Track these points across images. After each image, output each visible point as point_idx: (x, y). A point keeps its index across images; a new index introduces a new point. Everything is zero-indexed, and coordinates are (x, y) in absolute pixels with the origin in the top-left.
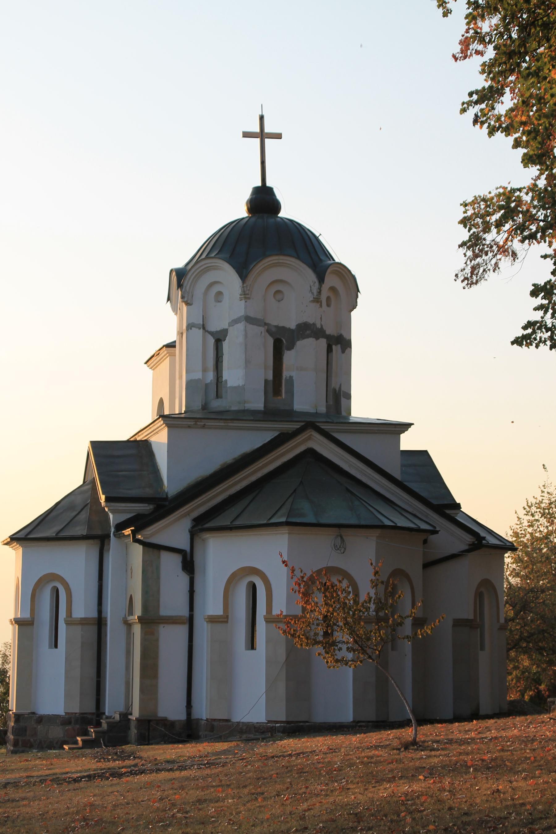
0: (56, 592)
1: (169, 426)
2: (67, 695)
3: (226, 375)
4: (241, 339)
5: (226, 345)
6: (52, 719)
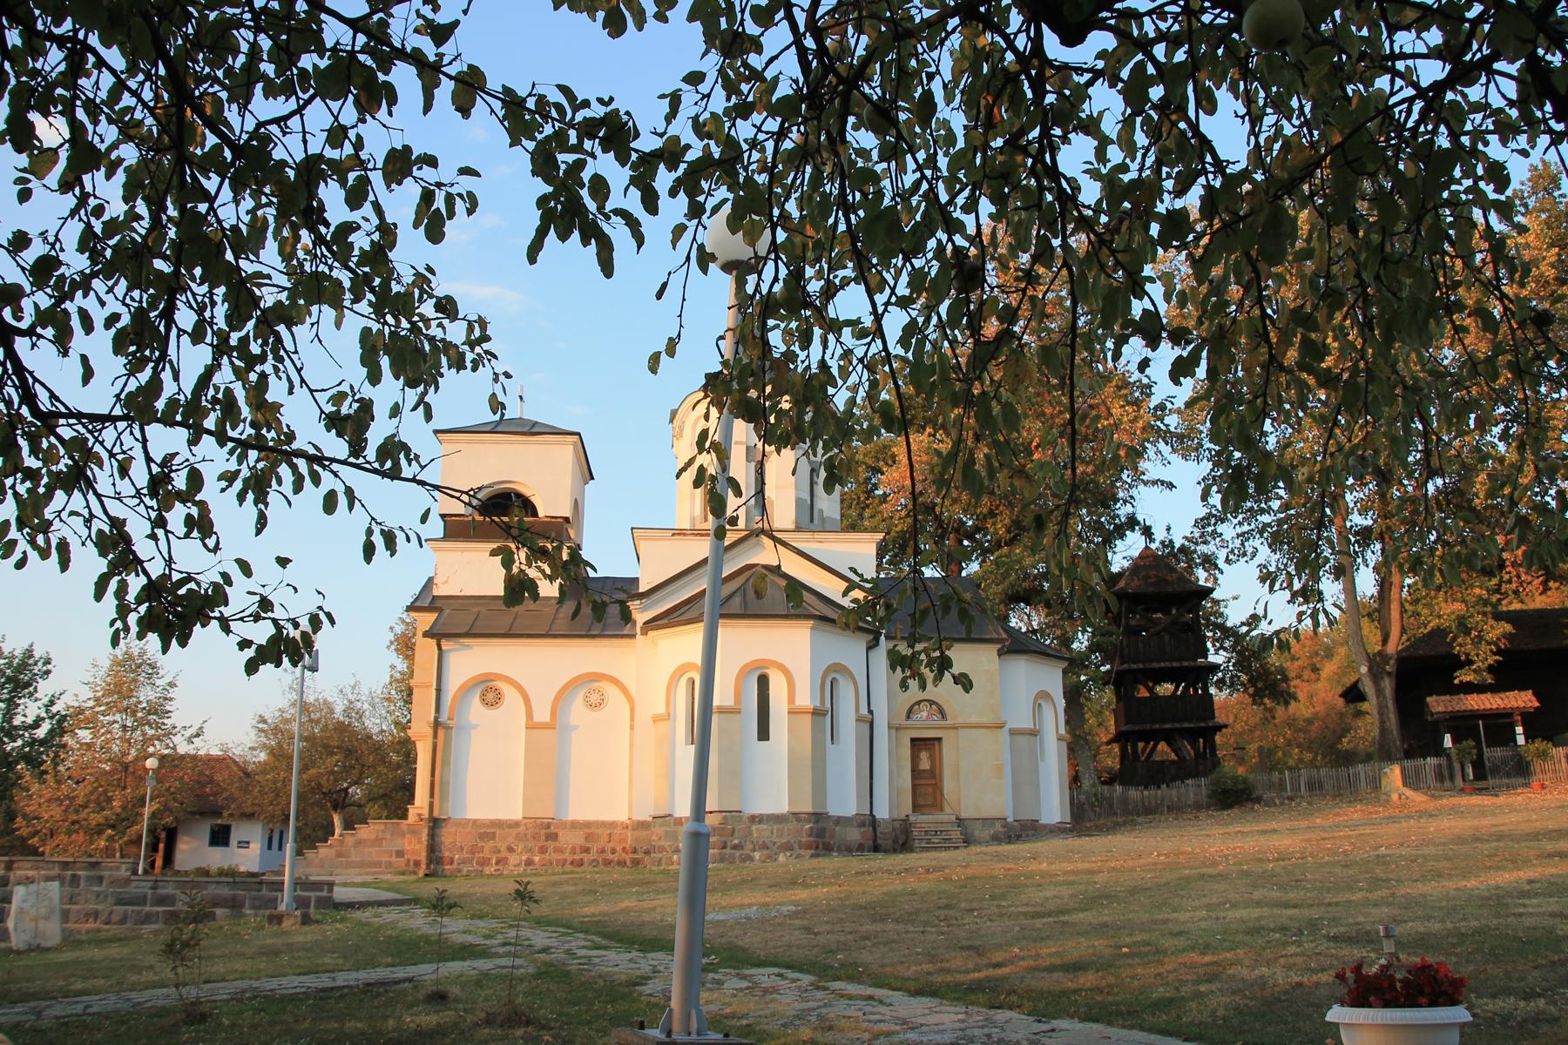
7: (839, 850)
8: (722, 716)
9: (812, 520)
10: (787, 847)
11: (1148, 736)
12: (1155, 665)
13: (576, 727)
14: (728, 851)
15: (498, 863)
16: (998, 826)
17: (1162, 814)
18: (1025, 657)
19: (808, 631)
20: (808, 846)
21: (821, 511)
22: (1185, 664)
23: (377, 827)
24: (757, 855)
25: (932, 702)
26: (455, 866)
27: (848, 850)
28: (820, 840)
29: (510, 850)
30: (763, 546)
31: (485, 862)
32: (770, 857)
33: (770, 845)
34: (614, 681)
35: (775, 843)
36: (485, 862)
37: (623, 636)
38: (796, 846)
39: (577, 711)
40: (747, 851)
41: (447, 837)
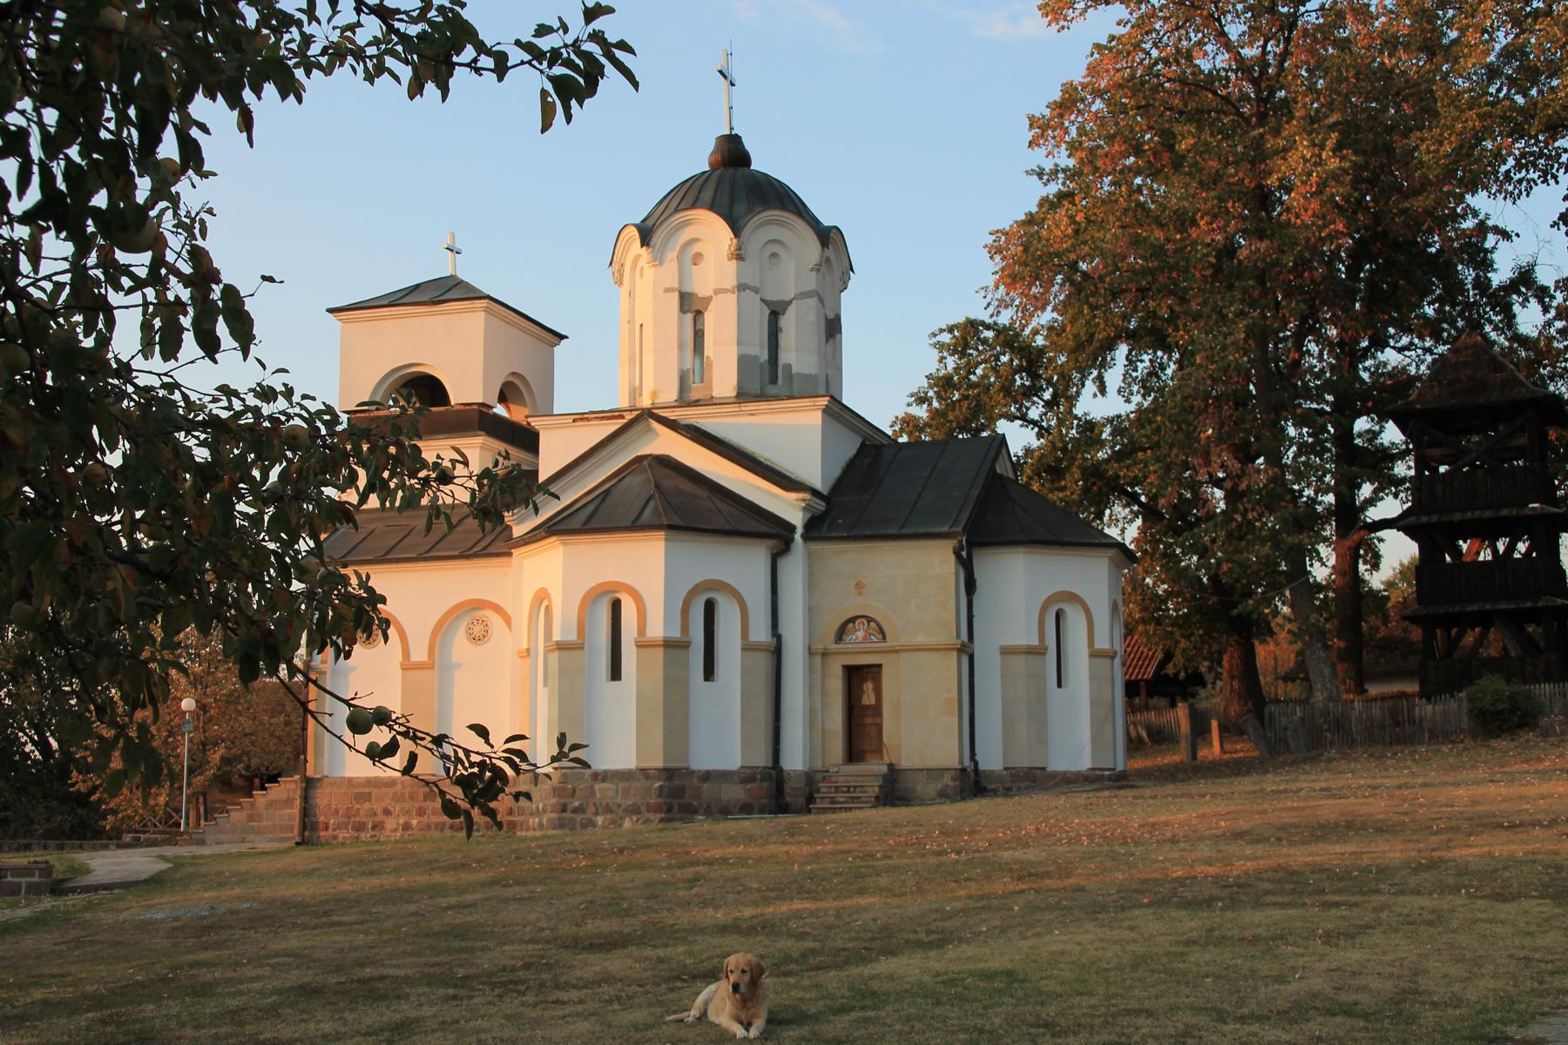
0: (710, 607)
1: (826, 411)
2: (746, 743)
3: (785, 357)
4: (812, 317)
5: (788, 322)
6: (724, 776)
7: (708, 812)
8: (563, 652)
9: (774, 380)
10: (634, 810)
11: (1447, 621)
12: (1457, 517)
13: (458, 666)
14: (567, 815)
15: (374, 828)
16: (947, 780)
17: (1421, 743)
18: (1021, 549)
19: (662, 543)
20: (657, 809)
21: (788, 367)
22: (1504, 512)
23: (287, 786)
24: (600, 820)
25: (870, 620)
26: (330, 832)
27: (725, 811)
28: (675, 802)
29: (387, 812)
30: (650, 429)
31: (360, 827)
32: (613, 822)
33: (615, 809)
34: (497, 608)
35: (619, 806)
36: (360, 827)
37: (498, 555)
38: (643, 809)
39: (460, 646)
40: (588, 815)
41: (322, 798)
